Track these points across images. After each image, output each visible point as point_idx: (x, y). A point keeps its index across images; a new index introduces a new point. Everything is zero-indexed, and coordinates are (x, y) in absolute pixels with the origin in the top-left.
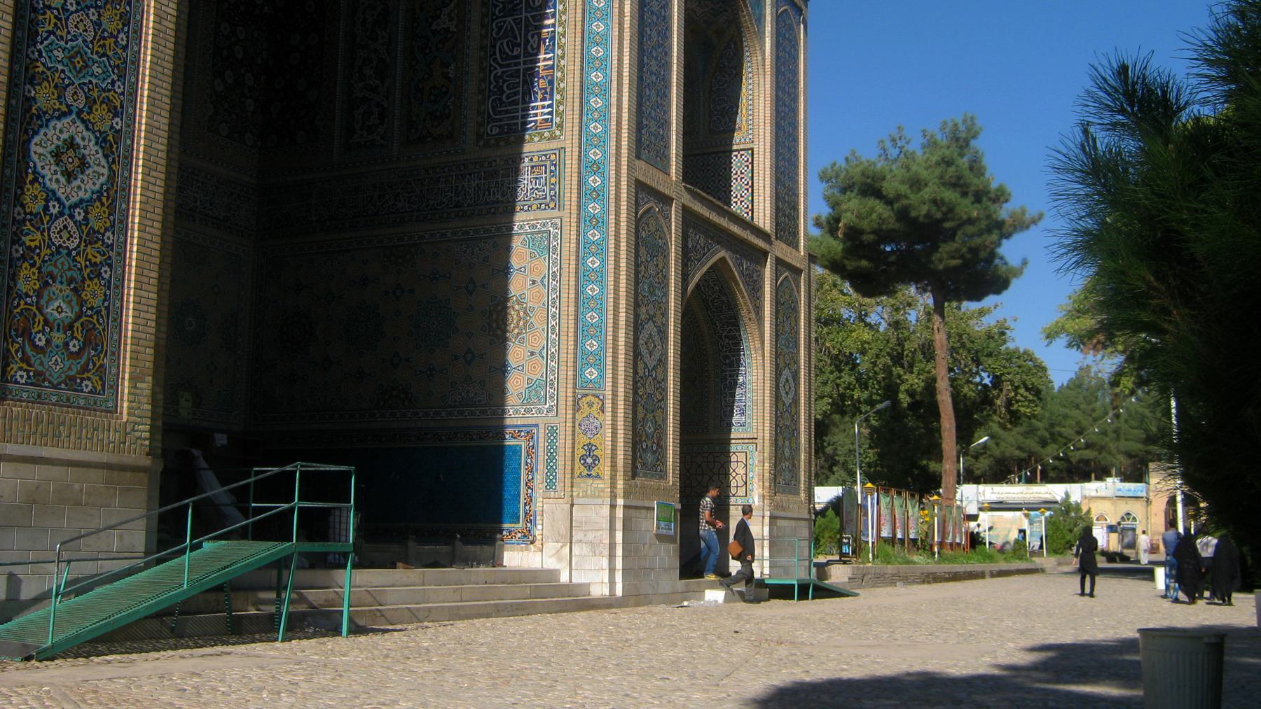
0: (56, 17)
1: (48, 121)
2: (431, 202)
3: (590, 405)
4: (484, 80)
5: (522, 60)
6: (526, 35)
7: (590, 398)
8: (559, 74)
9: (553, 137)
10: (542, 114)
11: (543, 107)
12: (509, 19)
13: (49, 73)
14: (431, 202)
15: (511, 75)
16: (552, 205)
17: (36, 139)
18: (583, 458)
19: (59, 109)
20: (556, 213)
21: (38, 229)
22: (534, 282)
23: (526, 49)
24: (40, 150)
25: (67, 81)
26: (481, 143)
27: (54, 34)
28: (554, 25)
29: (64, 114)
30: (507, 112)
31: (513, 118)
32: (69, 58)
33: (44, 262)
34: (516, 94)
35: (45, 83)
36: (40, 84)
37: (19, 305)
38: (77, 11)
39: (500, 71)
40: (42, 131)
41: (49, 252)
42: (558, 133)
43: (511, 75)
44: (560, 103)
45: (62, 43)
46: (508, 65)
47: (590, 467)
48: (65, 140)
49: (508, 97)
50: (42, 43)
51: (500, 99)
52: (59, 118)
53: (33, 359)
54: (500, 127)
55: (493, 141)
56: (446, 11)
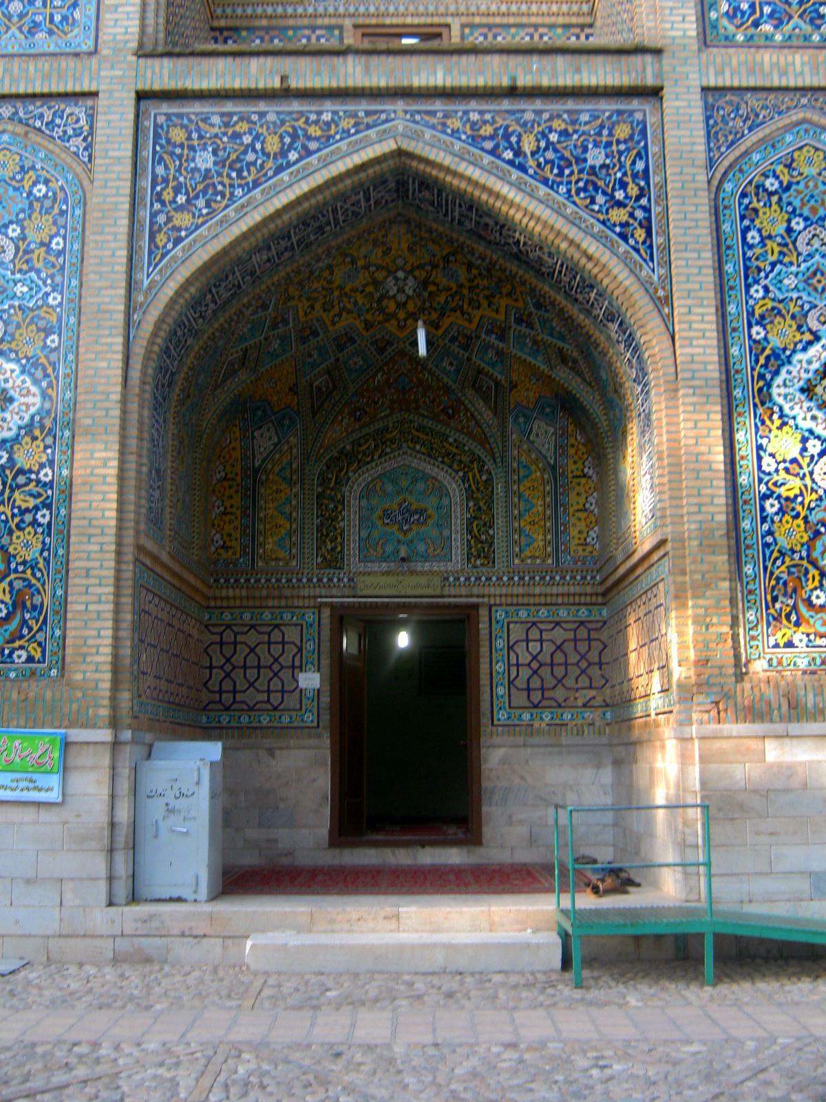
0: (779, 244)
1: (789, 357)
13: (781, 306)
17: (779, 380)
19: (801, 341)
21: (797, 475)
24: (782, 391)
25: (807, 307)
27: (781, 262)
29: (810, 343)
32: (805, 281)
33: (811, 510)
35: (778, 319)
36: (772, 322)
37: (783, 563)
38: (805, 228)
40: (784, 371)
41: (814, 496)
45: (794, 269)
48: (816, 371)
50: (767, 277)
52: (804, 349)
53: (812, 621)
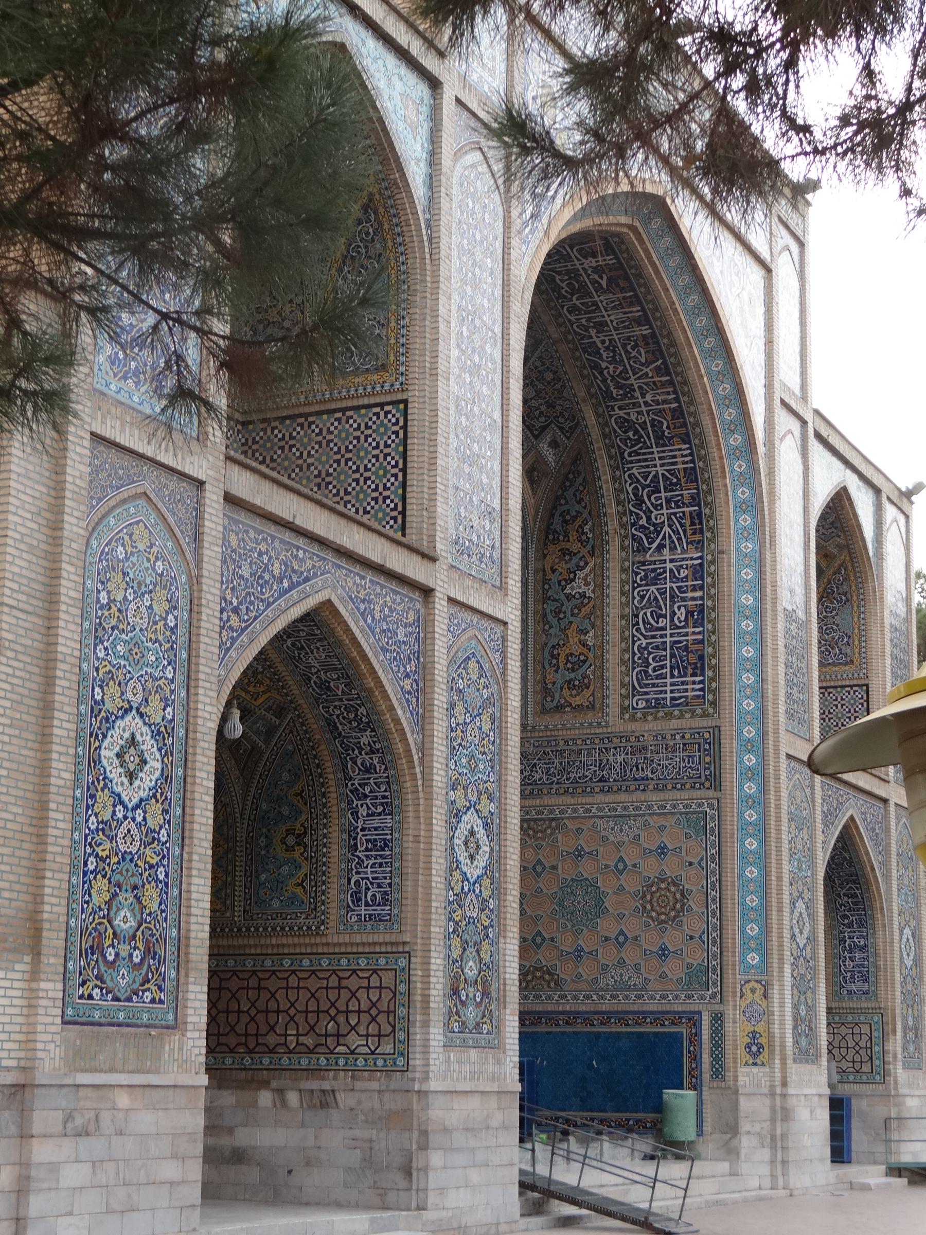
2: (572, 775)
3: (753, 991)
4: (627, 651)
5: (668, 632)
6: (672, 607)
7: (753, 984)
8: (710, 650)
9: (705, 715)
10: (693, 690)
11: (694, 683)
12: (653, 588)
14: (572, 775)
15: (657, 648)
16: (707, 784)
18: (748, 1046)
20: (711, 793)
22: (691, 864)
23: (672, 620)
26: (627, 716)
28: (702, 598)
30: (653, 685)
31: (661, 692)
34: (662, 667)
39: (644, 642)
42: (711, 710)
43: (657, 648)
44: (712, 679)
46: (654, 637)
47: (755, 1055)
49: (654, 670)
51: (646, 672)
54: (647, 701)
55: (639, 715)
56: (581, 574)
